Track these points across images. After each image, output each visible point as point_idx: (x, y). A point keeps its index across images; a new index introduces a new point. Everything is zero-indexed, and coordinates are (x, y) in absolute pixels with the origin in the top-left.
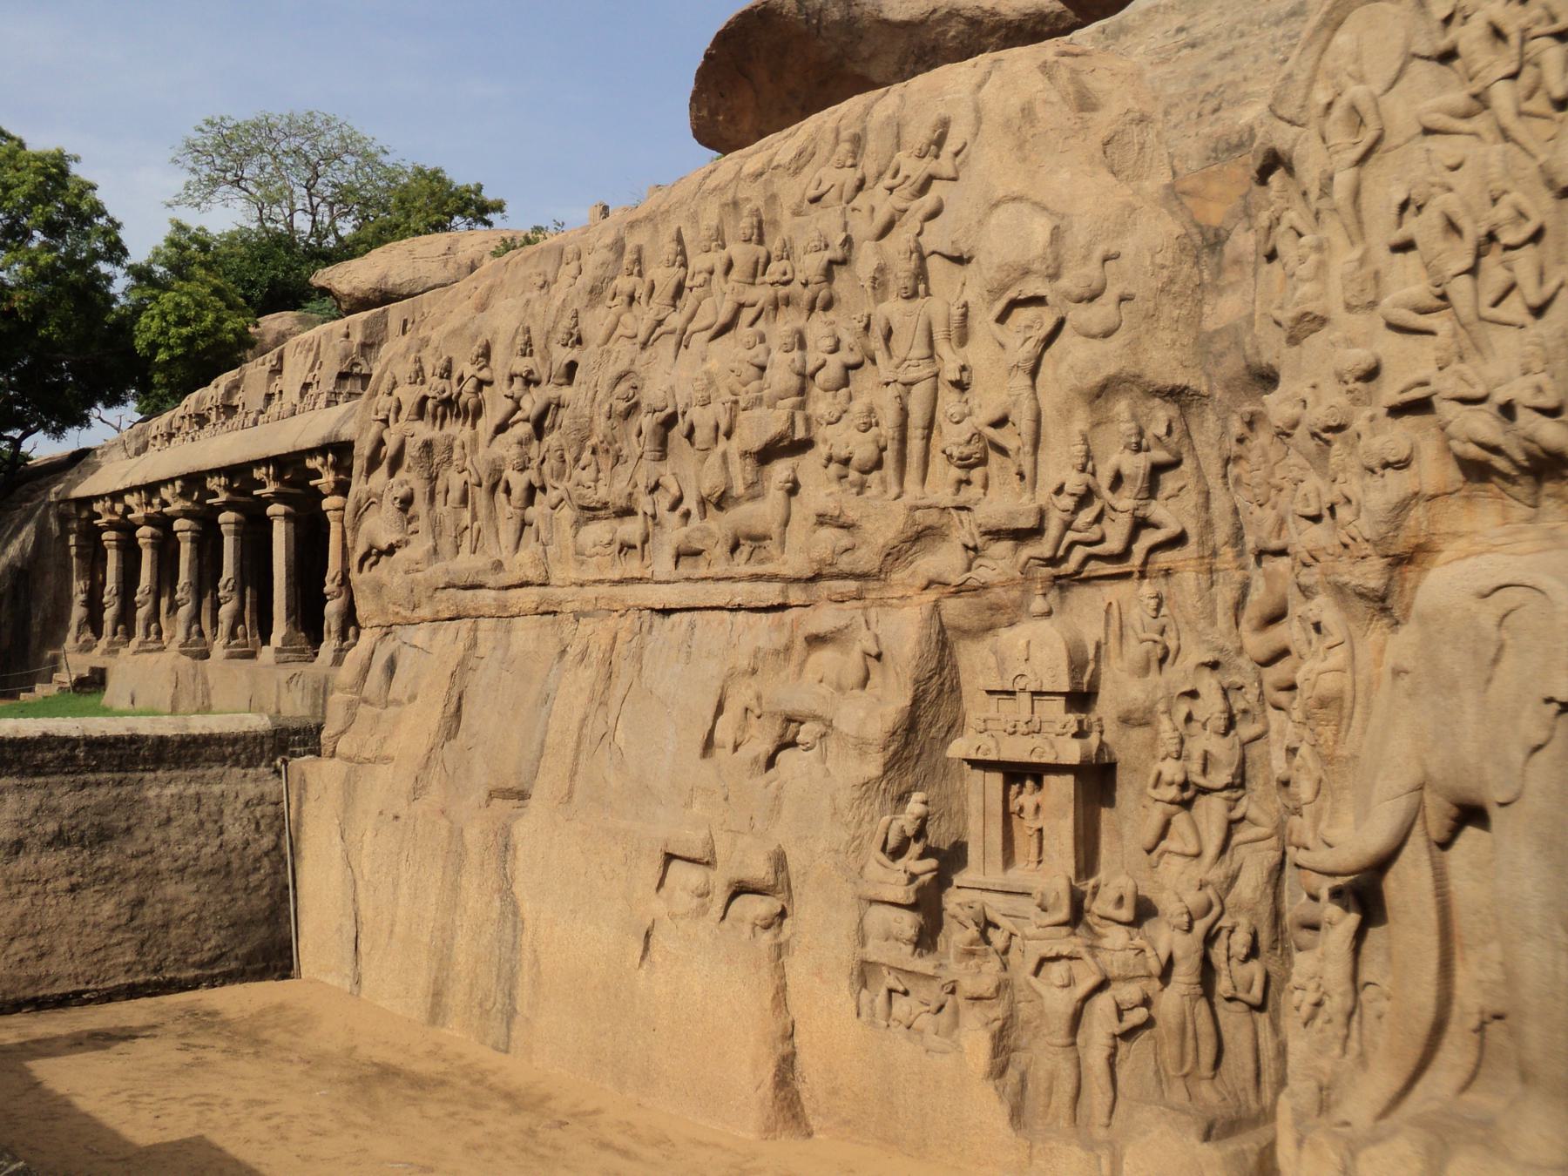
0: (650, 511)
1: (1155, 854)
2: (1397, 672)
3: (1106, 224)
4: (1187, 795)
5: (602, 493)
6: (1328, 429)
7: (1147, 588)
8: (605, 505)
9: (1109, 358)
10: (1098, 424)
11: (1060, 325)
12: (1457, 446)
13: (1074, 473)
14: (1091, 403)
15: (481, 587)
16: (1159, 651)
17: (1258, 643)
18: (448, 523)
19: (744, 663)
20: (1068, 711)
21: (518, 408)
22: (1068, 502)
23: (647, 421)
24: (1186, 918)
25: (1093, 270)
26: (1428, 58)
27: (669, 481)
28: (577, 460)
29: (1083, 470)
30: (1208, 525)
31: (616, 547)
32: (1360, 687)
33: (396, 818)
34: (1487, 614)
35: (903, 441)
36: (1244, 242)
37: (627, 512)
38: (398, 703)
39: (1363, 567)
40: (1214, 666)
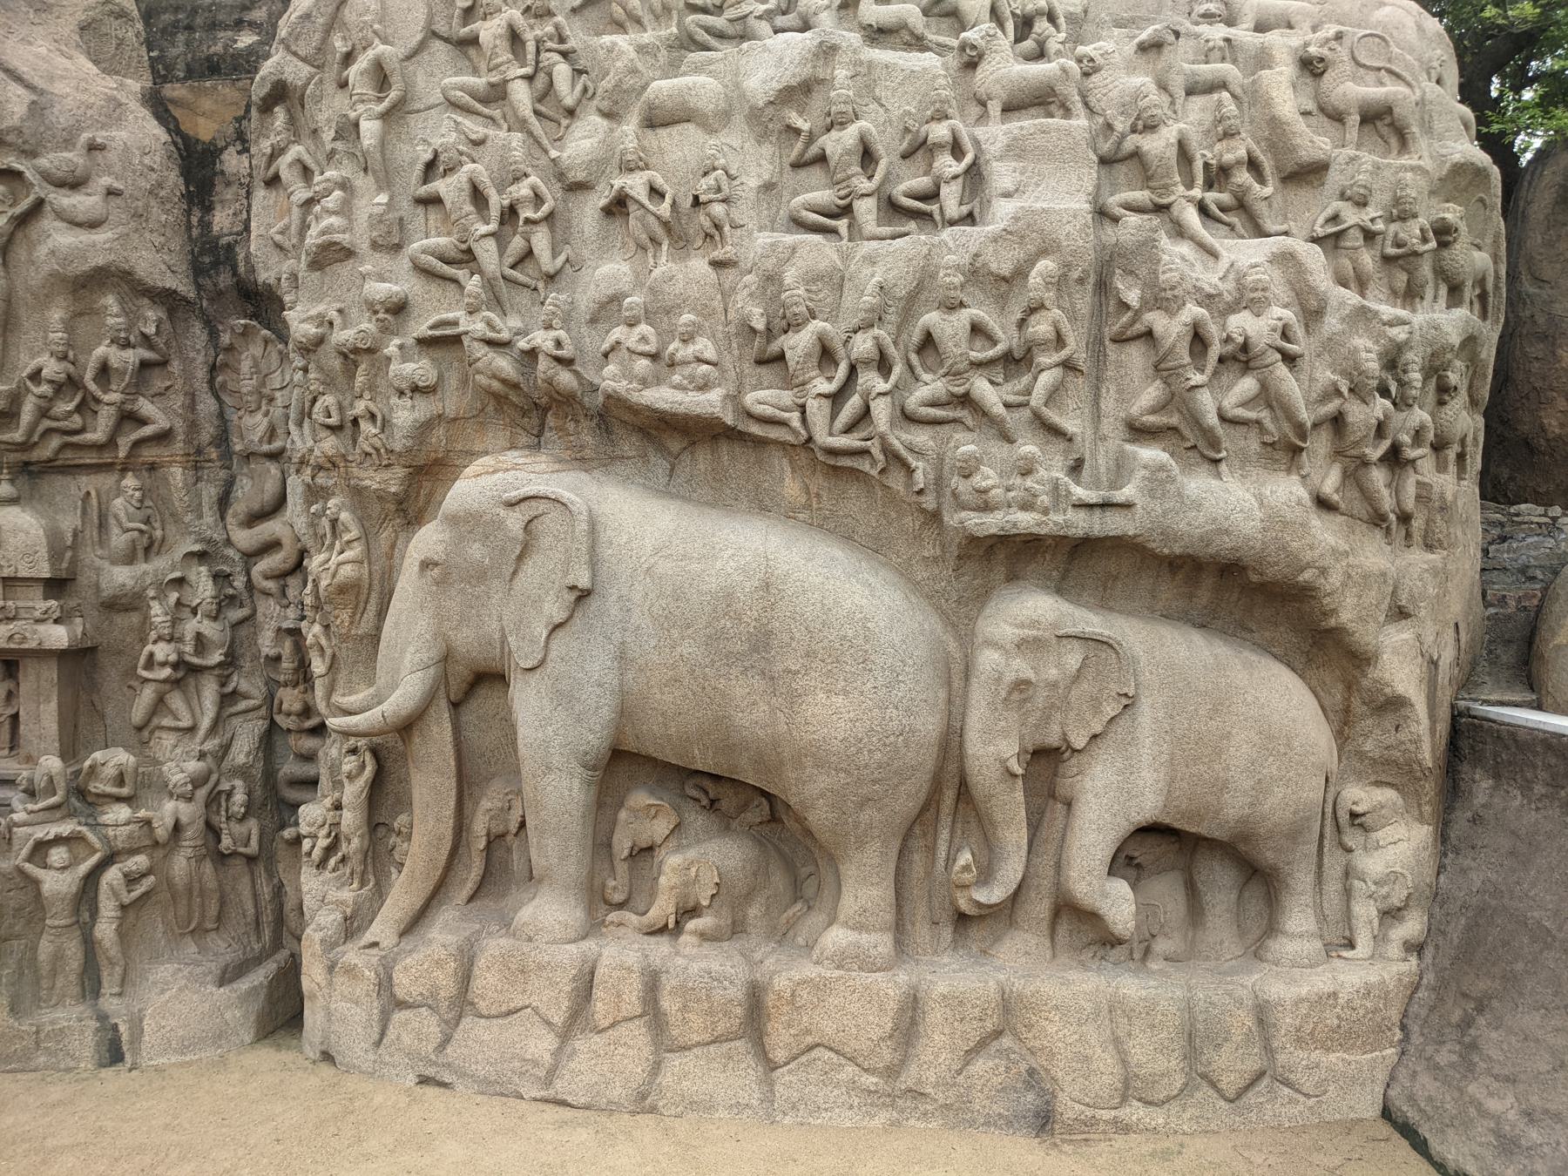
1: (146, 733)
2: (426, 565)
3: (89, 112)
4: (180, 674)
6: (356, 351)
7: (130, 481)
9: (99, 247)
10: (81, 314)
11: (39, 204)
12: (482, 380)
13: (53, 360)
14: (74, 291)
16: (145, 541)
17: (245, 538)
20: (46, 598)
24: (190, 787)
25: (74, 158)
26: (446, 40)
29: (64, 358)
30: (193, 426)
32: (376, 576)
34: (514, 521)
36: (232, 162)
39: (386, 475)
40: (202, 556)
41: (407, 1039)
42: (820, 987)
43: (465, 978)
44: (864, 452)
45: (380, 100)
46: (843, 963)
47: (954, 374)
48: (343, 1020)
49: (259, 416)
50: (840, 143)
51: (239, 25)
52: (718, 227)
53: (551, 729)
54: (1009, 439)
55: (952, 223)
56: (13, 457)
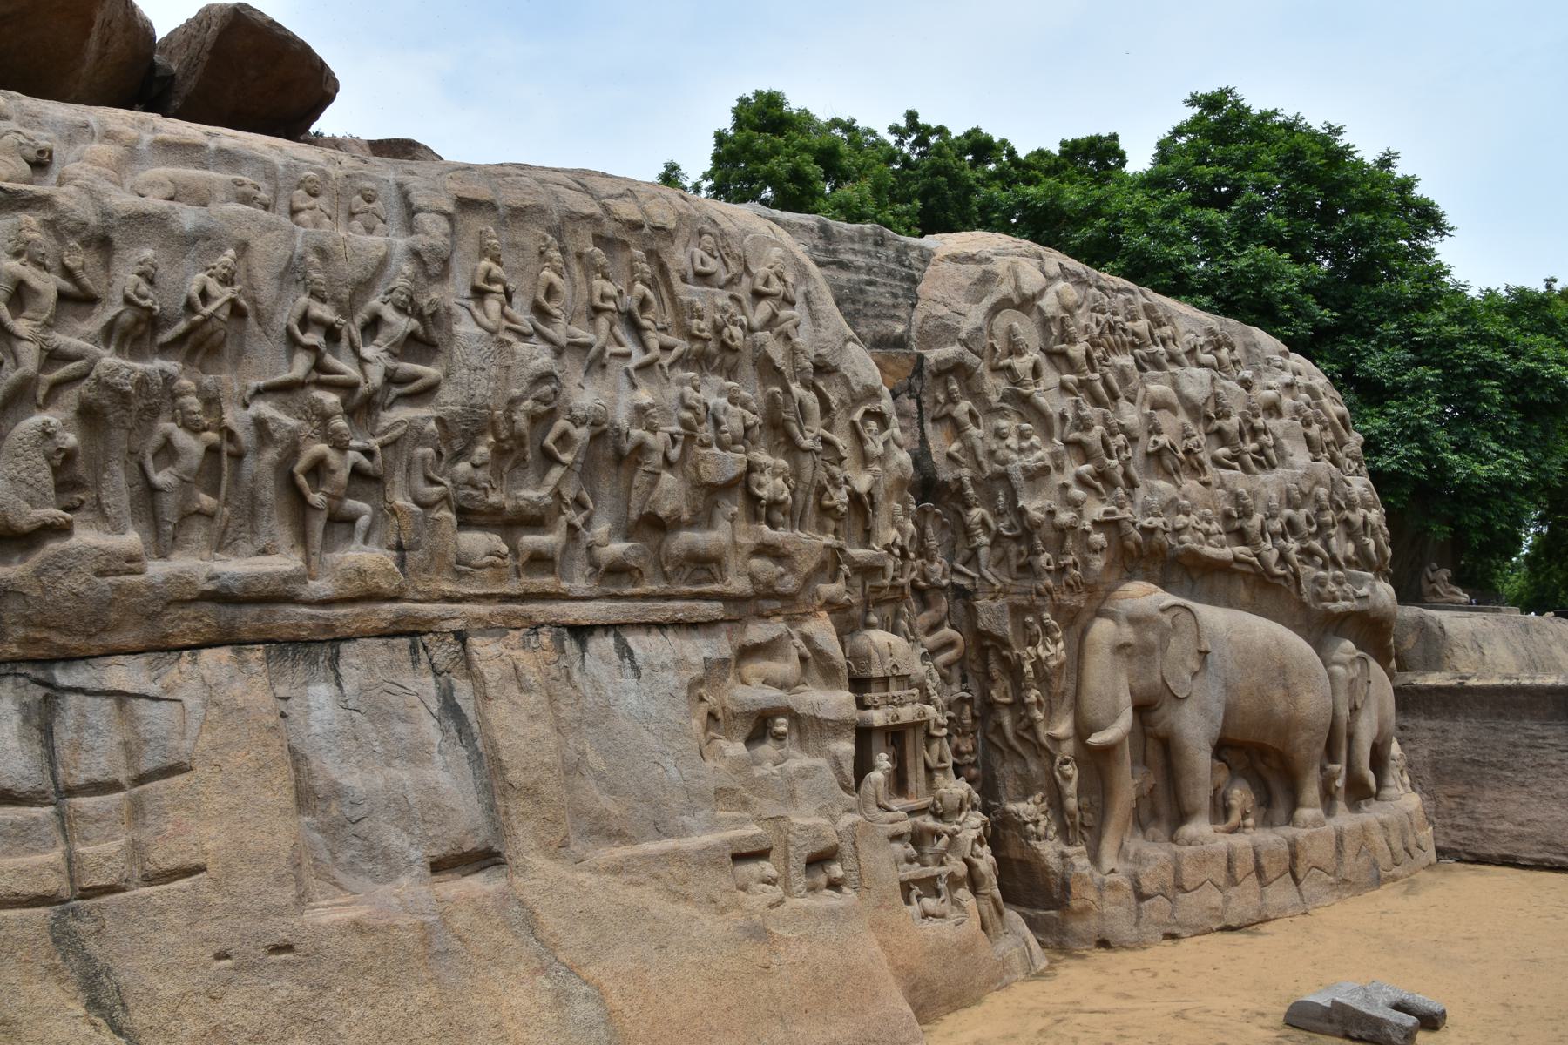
0: (578, 522)
5: (494, 498)
8: (498, 510)
12: (1130, 544)
15: (292, 600)
18: (169, 506)
19: (698, 672)
21: (319, 366)
22: (897, 552)
23: (581, 434)
27: (586, 495)
28: (458, 456)
31: (523, 558)
33: (288, 948)
35: (807, 494)
37: (537, 522)
38: (115, 786)
41: (1154, 915)
42: (1310, 838)
43: (1177, 872)
44: (1284, 577)
45: (1036, 384)
46: (1316, 825)
47: (1302, 539)
48: (1113, 917)
49: (936, 565)
50: (1232, 424)
51: (892, 317)
52: (1201, 464)
53: (1196, 728)
54: (1324, 567)
55: (1273, 467)
56: (873, 597)
